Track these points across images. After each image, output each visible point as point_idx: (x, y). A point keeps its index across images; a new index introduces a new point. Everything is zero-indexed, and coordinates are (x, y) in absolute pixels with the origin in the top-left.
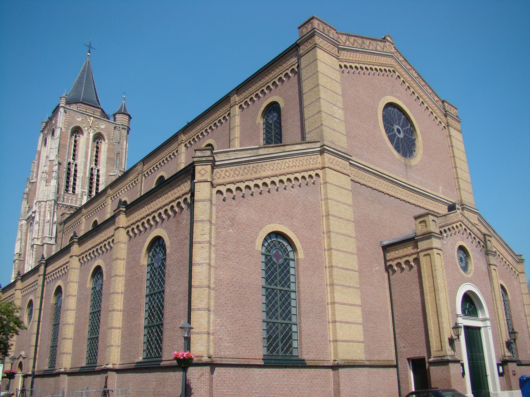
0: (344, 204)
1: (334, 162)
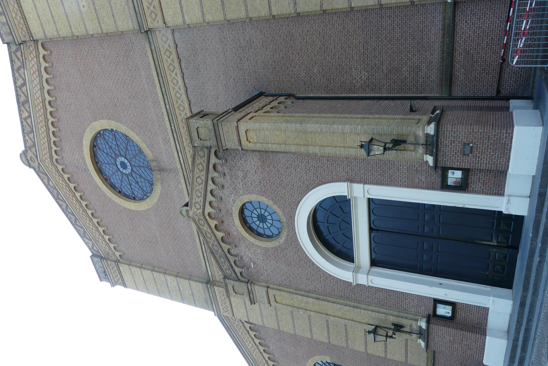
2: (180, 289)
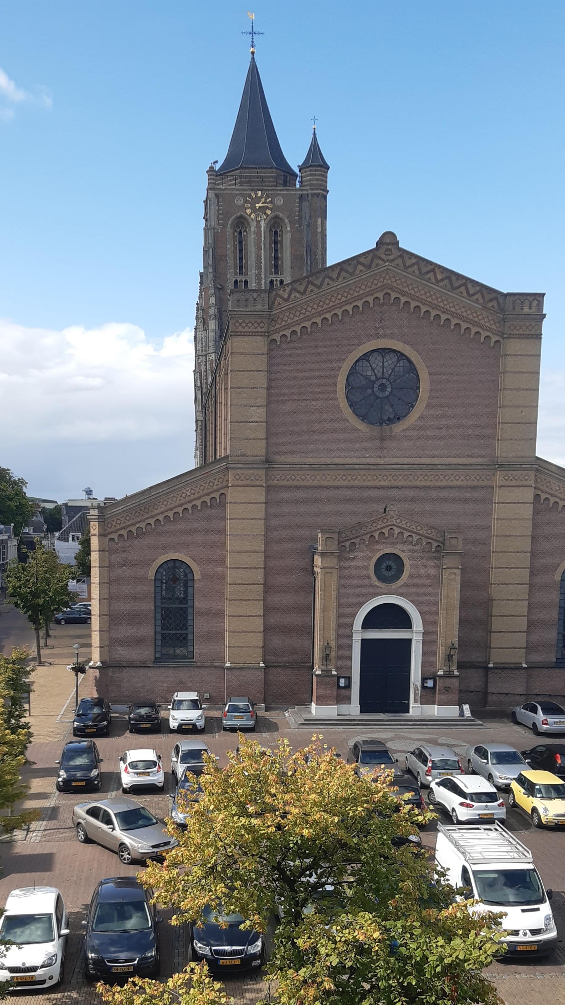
0: (252, 519)
1: (243, 477)
2: (250, 422)
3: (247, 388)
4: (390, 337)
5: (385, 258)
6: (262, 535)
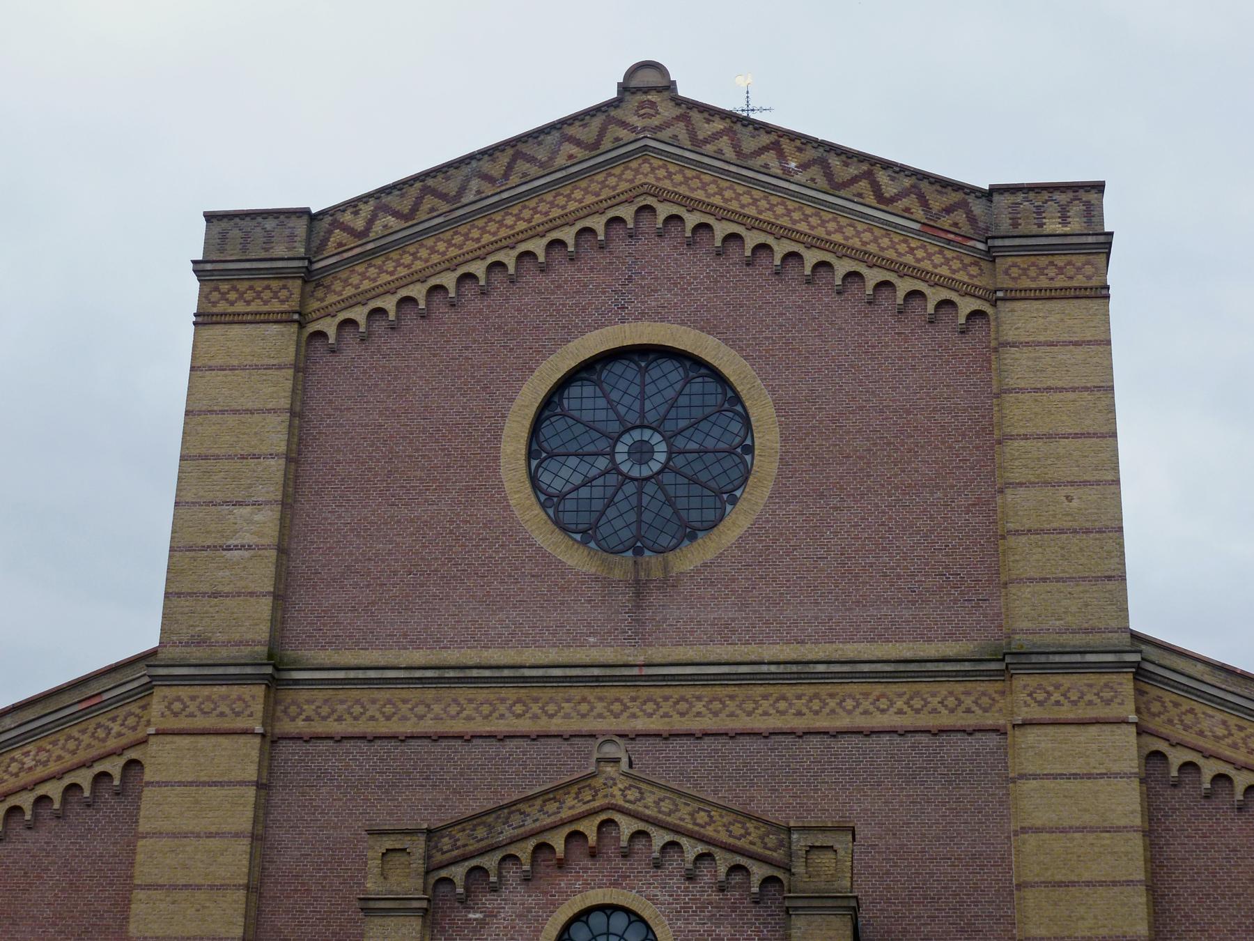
0: (210, 835)
1: (192, 707)
2: (229, 549)
3: (230, 457)
4: (659, 315)
5: (639, 123)
6: (237, 887)
